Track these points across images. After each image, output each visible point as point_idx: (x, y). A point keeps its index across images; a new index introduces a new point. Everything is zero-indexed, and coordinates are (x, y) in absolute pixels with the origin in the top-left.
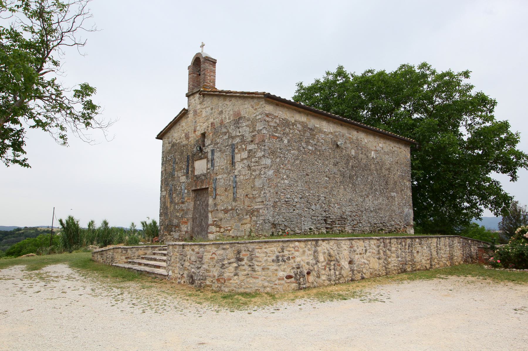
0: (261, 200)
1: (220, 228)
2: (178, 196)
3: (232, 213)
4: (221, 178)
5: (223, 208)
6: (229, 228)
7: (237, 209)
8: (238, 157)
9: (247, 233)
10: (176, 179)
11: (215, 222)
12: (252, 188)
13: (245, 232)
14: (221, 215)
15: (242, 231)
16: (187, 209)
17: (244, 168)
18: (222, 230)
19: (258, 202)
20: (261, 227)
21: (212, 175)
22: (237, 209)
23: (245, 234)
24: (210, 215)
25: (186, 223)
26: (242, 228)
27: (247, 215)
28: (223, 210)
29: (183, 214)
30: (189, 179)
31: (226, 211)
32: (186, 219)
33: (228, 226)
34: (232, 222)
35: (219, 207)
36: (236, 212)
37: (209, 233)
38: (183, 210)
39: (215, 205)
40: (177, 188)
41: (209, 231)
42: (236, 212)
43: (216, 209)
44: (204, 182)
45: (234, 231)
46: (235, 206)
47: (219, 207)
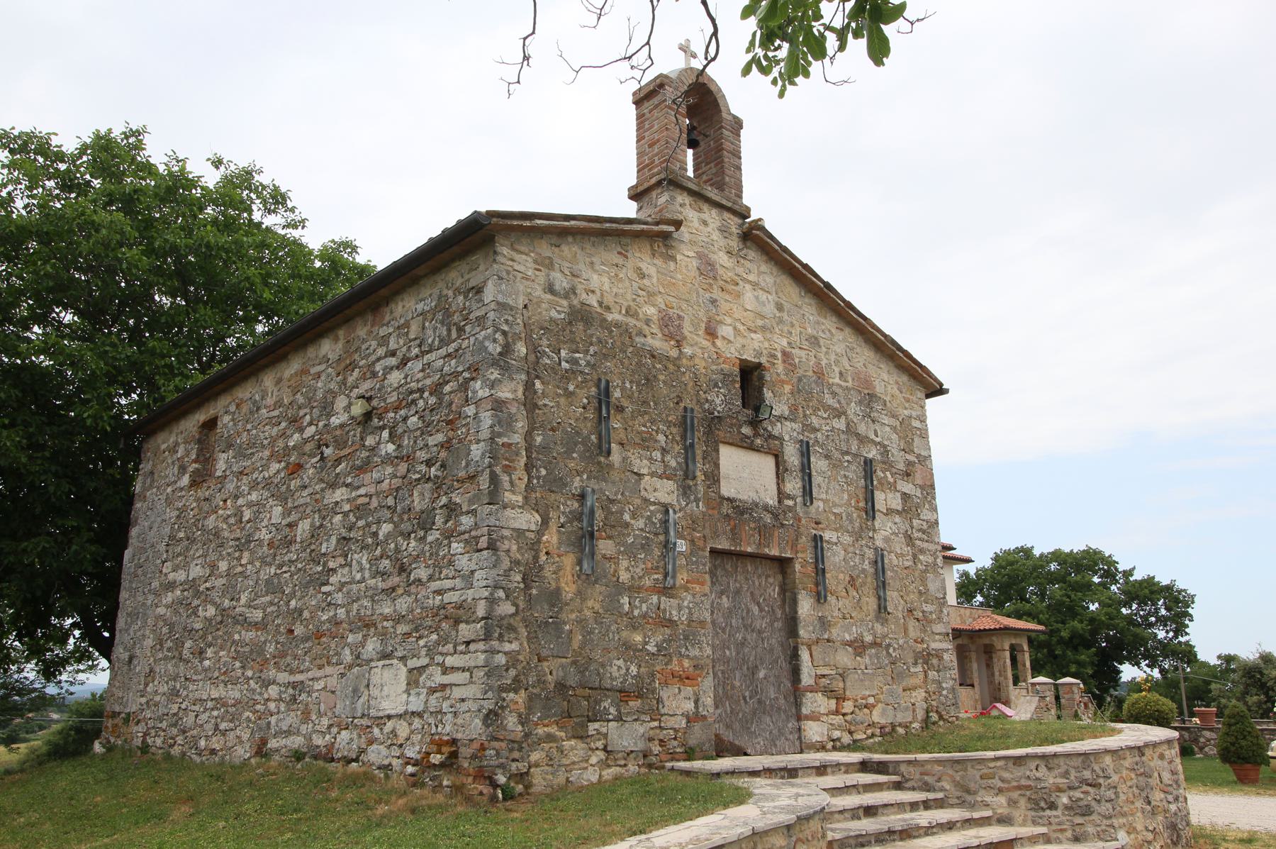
0: (944, 631)
1: (840, 699)
2: (632, 556)
3: (876, 654)
4: (835, 540)
5: (847, 637)
6: (871, 700)
7: (889, 645)
8: (883, 499)
9: (920, 714)
10: (615, 475)
11: (824, 681)
12: (920, 592)
13: (914, 711)
14: (845, 659)
15: (907, 709)
16: (691, 621)
17: (896, 535)
18: (848, 706)
19: (939, 634)
20: (950, 696)
21: (803, 521)
22: (889, 645)
23: (914, 717)
24: (804, 655)
25: (685, 679)
26: (905, 700)
27: (915, 664)
28: (850, 644)
29: (669, 641)
30: (697, 500)
31: (859, 647)
32: (686, 663)
33: (867, 693)
34: (879, 681)
35: (835, 632)
36: (888, 652)
37: (808, 718)
38: (671, 623)
39: (824, 623)
40: (627, 517)
41: (805, 711)
42: (888, 652)
43: (826, 637)
44: (771, 535)
45: (884, 710)
46: (885, 637)
47: (835, 632)
